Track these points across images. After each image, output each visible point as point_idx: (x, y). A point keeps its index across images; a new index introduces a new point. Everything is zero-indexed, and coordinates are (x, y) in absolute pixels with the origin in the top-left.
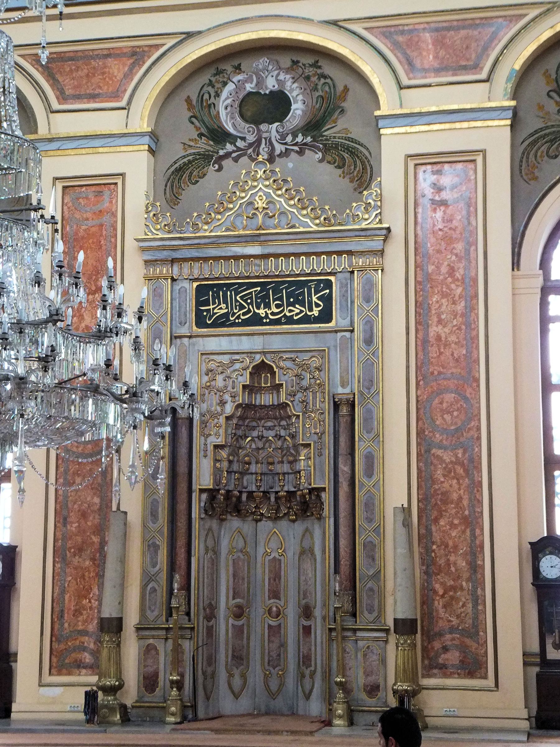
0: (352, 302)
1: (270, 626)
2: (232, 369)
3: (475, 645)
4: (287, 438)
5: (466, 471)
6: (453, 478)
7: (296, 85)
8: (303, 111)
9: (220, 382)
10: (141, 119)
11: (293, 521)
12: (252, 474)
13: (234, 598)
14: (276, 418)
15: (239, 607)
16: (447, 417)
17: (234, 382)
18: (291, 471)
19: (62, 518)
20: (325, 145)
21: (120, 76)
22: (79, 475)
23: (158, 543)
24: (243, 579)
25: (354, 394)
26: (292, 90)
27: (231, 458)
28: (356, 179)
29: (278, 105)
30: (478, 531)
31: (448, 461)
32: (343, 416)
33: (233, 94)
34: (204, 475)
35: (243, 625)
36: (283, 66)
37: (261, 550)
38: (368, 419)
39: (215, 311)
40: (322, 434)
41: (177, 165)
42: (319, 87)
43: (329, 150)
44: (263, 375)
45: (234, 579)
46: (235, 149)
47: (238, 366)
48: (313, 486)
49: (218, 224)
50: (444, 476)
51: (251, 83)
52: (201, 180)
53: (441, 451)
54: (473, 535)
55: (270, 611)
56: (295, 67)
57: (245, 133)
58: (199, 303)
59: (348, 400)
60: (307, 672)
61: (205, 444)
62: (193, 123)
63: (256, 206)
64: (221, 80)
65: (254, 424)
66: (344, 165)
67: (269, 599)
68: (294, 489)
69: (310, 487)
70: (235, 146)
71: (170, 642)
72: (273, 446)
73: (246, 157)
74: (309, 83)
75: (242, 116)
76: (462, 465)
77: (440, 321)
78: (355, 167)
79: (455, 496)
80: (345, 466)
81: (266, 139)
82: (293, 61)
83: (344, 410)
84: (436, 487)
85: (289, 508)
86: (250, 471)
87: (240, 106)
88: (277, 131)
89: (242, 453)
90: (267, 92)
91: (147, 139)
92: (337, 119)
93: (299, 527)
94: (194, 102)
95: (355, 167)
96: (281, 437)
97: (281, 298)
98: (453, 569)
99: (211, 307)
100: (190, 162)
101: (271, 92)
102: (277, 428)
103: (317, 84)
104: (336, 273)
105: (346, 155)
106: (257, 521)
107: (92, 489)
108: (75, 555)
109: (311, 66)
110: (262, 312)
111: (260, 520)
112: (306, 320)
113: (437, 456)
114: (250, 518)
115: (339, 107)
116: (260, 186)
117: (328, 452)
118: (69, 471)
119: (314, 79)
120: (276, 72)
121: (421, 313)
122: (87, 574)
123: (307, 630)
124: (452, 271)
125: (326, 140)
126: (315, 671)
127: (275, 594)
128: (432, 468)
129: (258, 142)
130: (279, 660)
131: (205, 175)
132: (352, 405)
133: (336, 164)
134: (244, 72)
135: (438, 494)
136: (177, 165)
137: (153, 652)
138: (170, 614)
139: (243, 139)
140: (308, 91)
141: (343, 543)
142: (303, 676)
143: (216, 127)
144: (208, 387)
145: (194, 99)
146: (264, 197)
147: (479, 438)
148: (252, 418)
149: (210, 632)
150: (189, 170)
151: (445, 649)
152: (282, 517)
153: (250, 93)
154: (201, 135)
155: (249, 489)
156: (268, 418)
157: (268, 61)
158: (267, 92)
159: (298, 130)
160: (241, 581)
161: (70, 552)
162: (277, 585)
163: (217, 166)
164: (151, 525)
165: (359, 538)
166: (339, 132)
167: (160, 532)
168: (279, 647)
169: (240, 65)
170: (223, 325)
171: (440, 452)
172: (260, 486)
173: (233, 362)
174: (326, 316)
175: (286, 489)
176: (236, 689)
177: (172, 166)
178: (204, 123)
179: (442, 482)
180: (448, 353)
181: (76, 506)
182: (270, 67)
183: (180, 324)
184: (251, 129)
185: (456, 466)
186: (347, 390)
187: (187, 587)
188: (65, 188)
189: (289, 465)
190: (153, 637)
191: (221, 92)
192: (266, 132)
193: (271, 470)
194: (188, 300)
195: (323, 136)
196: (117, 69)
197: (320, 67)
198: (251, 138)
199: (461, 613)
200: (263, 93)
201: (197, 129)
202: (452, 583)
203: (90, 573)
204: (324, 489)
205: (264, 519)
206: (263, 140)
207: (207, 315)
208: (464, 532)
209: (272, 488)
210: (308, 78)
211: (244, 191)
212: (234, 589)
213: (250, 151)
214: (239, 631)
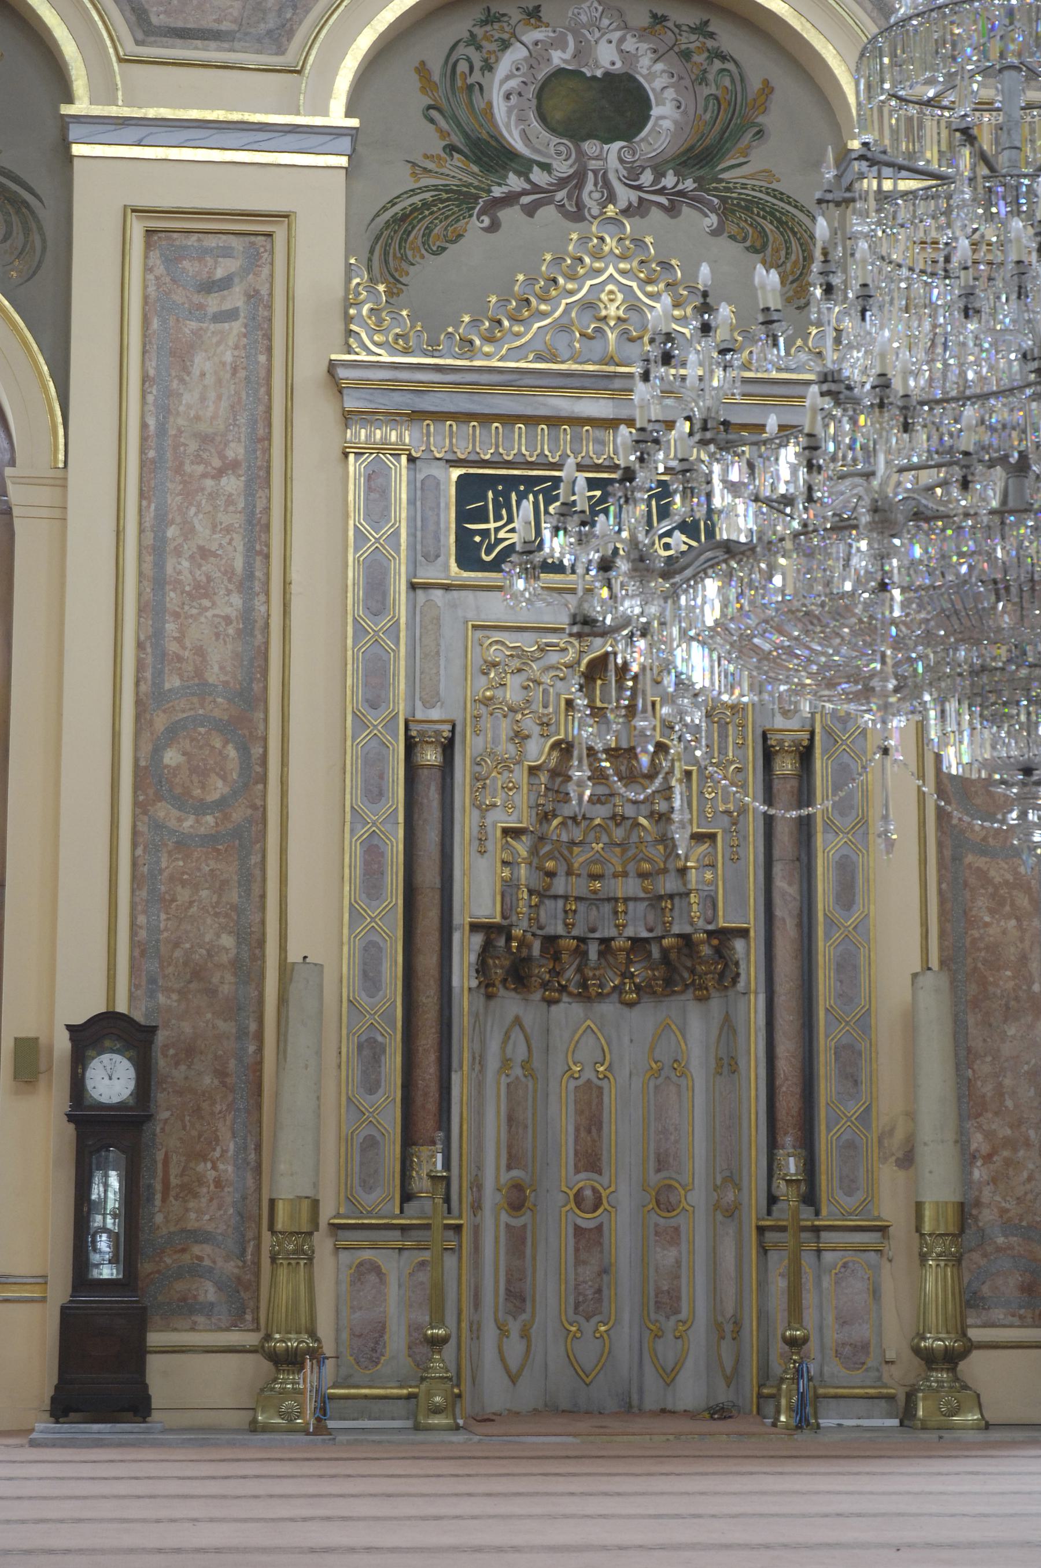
1: (579, 1231)
2: (542, 663)
4: (642, 821)
6: (1008, 917)
7: (660, 66)
8: (676, 122)
11: (631, 1005)
12: (556, 897)
13: (509, 1168)
15: (518, 1187)
17: (545, 692)
18: (642, 895)
20: (723, 200)
22: (184, 884)
23: (380, 1039)
24: (526, 1127)
25: (812, 733)
26: (651, 77)
28: (791, 278)
31: (998, 880)
32: (785, 777)
33: (524, 69)
35: (525, 1226)
36: (630, 25)
39: (502, 535)
41: (397, 209)
42: (711, 77)
43: (733, 212)
44: (599, 682)
45: (510, 1126)
46: (528, 187)
47: (554, 658)
48: (722, 924)
49: (518, 343)
50: (992, 911)
51: (564, 51)
52: (452, 247)
53: (984, 859)
56: (658, 27)
57: (551, 157)
58: (463, 516)
59: (797, 744)
61: (482, 827)
62: (432, 121)
63: (604, 313)
64: (497, 36)
66: (765, 246)
67: (577, 1171)
68: (645, 934)
69: (710, 927)
70: (528, 181)
73: (552, 207)
74: (689, 66)
75: (543, 118)
78: (788, 254)
79: (1011, 953)
80: (790, 884)
81: (595, 172)
82: (654, 16)
83: (786, 766)
84: (975, 933)
85: (623, 975)
86: (552, 892)
87: (540, 95)
88: (621, 161)
90: (599, 73)
91: (346, 143)
92: (749, 147)
94: (436, 77)
95: (788, 254)
96: (624, 818)
98: (1009, 1103)
99: (492, 525)
100: (426, 205)
101: (607, 74)
103: (705, 71)
105: (768, 227)
106: (550, 1002)
107: (217, 915)
108: (177, 1064)
109: (693, 30)
111: (557, 1002)
113: (978, 869)
115: (754, 124)
116: (611, 270)
118: (161, 871)
119: (699, 58)
120: (618, 34)
122: (205, 1105)
125: (727, 189)
127: (590, 1160)
128: (968, 894)
129: (578, 179)
130: (600, 1300)
131: (460, 236)
132: (805, 755)
133: (748, 244)
134: (547, 25)
135: (979, 950)
136: (397, 209)
137: (372, 1278)
138: (407, 1197)
139: (546, 167)
140: (687, 82)
141: (786, 1047)
143: (485, 136)
144: (487, 701)
145: (436, 69)
146: (620, 297)
150: (425, 223)
153: (560, 72)
154: (451, 149)
155: (550, 930)
157: (600, 9)
158: (599, 73)
159: (667, 162)
160: (520, 1131)
161: (165, 1056)
162: (594, 1141)
163: (487, 221)
165: (827, 1036)
166: (752, 176)
168: (599, 1275)
169: (538, 8)
171: (981, 862)
172: (573, 925)
175: (629, 932)
176: (514, 1365)
177: (385, 209)
178: (459, 125)
179: (987, 925)
181: (178, 953)
182: (605, 22)
183: (426, 556)
184: (562, 148)
185: (1015, 893)
188: (149, 232)
189: (638, 881)
191: (497, 61)
192: (597, 158)
193: (595, 892)
194: (442, 505)
195: (722, 180)
197: (711, 35)
198: (563, 168)
199: (1026, 1193)
200: (589, 74)
201: (443, 134)
202: (1009, 1132)
203: (213, 1103)
204: (744, 933)
205: (565, 998)
206: (590, 175)
207: (482, 542)
209: (593, 930)
210: (686, 55)
211: (571, 277)
212: (510, 1147)
213: (560, 195)
214: (517, 1242)
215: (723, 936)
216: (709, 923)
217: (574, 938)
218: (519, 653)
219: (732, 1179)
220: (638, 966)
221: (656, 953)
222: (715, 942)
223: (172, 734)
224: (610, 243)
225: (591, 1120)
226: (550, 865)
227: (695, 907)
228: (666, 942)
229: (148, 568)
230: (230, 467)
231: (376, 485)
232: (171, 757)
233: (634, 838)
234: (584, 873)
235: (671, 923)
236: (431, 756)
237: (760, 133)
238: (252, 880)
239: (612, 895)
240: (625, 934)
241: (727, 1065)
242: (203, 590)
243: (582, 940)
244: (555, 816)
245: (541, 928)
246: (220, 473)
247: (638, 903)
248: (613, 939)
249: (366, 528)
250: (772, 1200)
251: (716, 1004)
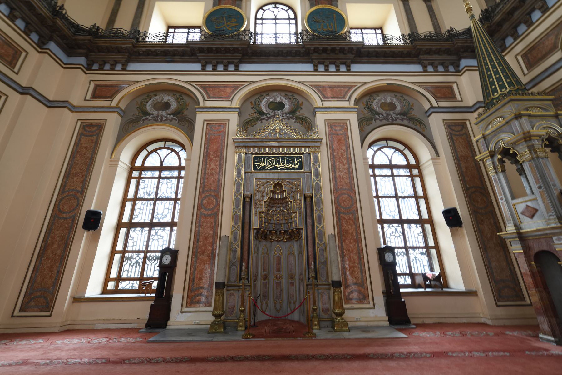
0: (310, 163)
3: (363, 290)
5: (354, 222)
9: (262, 189)
10: (236, 103)
15: (265, 275)
16: (345, 203)
19: (197, 239)
21: (229, 92)
29: (281, 106)
30: (360, 245)
34: (255, 223)
37: (272, 254)
38: (319, 202)
54: (358, 246)
55: (276, 277)
58: (254, 162)
59: (310, 196)
60: (292, 302)
71: (240, 292)
76: (352, 220)
77: (340, 171)
79: (350, 232)
83: (308, 200)
91: (238, 110)
93: (288, 244)
97: (284, 162)
106: (272, 242)
110: (277, 166)
112: (293, 169)
117: (303, 215)
121: (334, 169)
123: (292, 284)
124: (342, 155)
126: (296, 301)
127: (278, 270)
137: (233, 296)
138: (240, 279)
141: (310, 249)
142: (290, 303)
147: (357, 211)
149: (256, 286)
151: (352, 292)
154: (255, 112)
164: (234, 243)
167: (238, 245)
170: (263, 169)
171: (343, 215)
173: (267, 182)
174: (300, 168)
180: (343, 181)
186: (309, 193)
187: (247, 268)
190: (233, 290)
196: (228, 91)
198: (272, 114)
204: (302, 229)
208: (355, 245)
214: (265, 285)
215: (299, 230)
218: (263, 183)
219: (302, 274)
223: (205, 197)
224: (277, 121)
225: (279, 263)
229: (203, 172)
230: (217, 156)
231: (240, 158)
232: (205, 201)
236: (248, 200)
237: (302, 109)
238: (216, 222)
241: (300, 253)
242: (212, 175)
243: (276, 231)
246: (215, 157)
249: (238, 164)
250: (309, 279)
251: (299, 241)
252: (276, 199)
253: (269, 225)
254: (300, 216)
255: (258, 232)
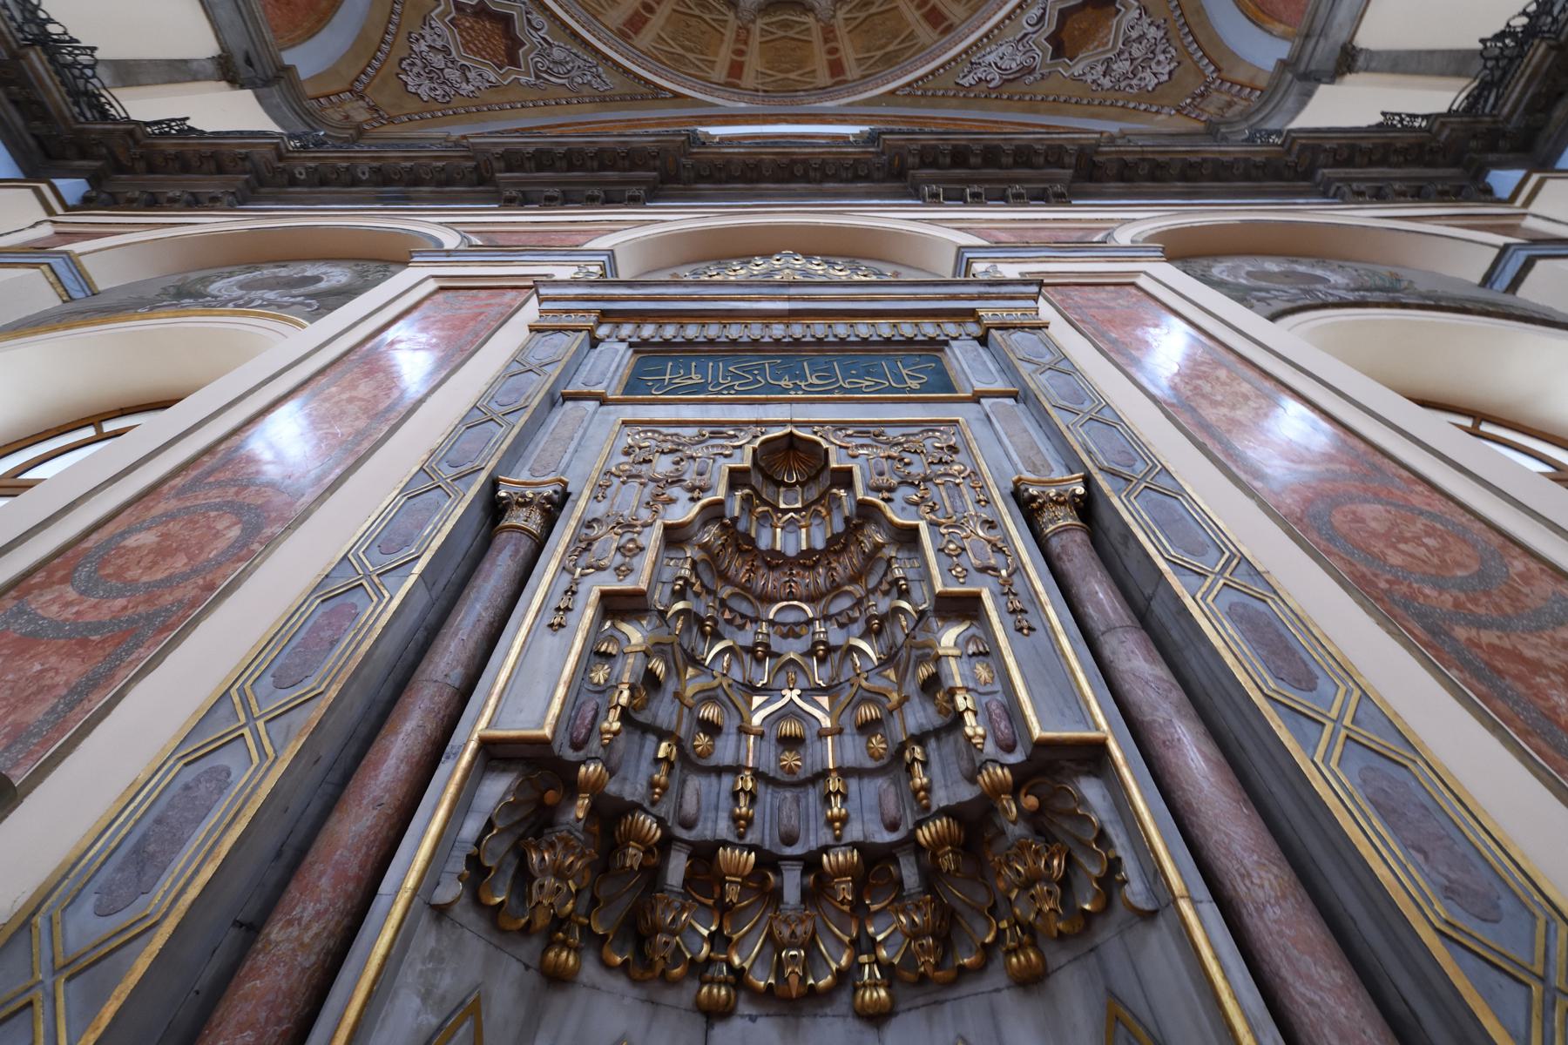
11: (876, 1018)
12: (719, 771)
14: (810, 599)
18: (870, 764)
27: (659, 667)
40: (1010, 575)
48: (1037, 732)
61: (571, 592)
65: (744, 607)
69: (1016, 757)
72: (803, 682)
86: (712, 762)
89: (693, 683)
96: (830, 649)
102: (817, 626)
104: (946, 343)
106: (714, 1014)
114: (685, 996)
132: (1088, 508)
148: (743, 587)
152: (830, 993)
156: (791, 596)
172: (749, 821)
175: (854, 832)
189: (861, 741)
193: (791, 771)
204: (1093, 756)
205: (744, 1008)
209: (789, 840)
216: (1010, 749)
217: (751, 848)
220: (881, 921)
221: (909, 873)
222: (1031, 801)
226: (709, 712)
227: (969, 718)
228: (924, 835)
233: (847, 673)
234: (772, 735)
235: (927, 789)
239: (818, 768)
240: (847, 839)
244: (717, 636)
245: (688, 825)
247: (866, 781)
248: (825, 849)
251: (1073, 990)
252: (775, 560)
253: (695, 783)
254: (1023, 620)
255: (532, 820)
